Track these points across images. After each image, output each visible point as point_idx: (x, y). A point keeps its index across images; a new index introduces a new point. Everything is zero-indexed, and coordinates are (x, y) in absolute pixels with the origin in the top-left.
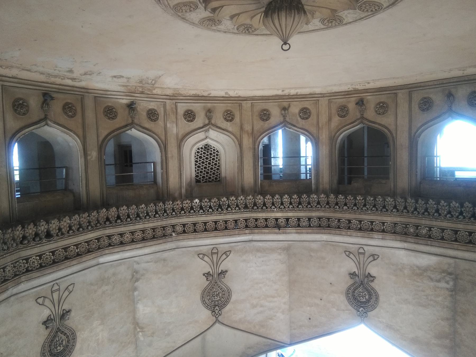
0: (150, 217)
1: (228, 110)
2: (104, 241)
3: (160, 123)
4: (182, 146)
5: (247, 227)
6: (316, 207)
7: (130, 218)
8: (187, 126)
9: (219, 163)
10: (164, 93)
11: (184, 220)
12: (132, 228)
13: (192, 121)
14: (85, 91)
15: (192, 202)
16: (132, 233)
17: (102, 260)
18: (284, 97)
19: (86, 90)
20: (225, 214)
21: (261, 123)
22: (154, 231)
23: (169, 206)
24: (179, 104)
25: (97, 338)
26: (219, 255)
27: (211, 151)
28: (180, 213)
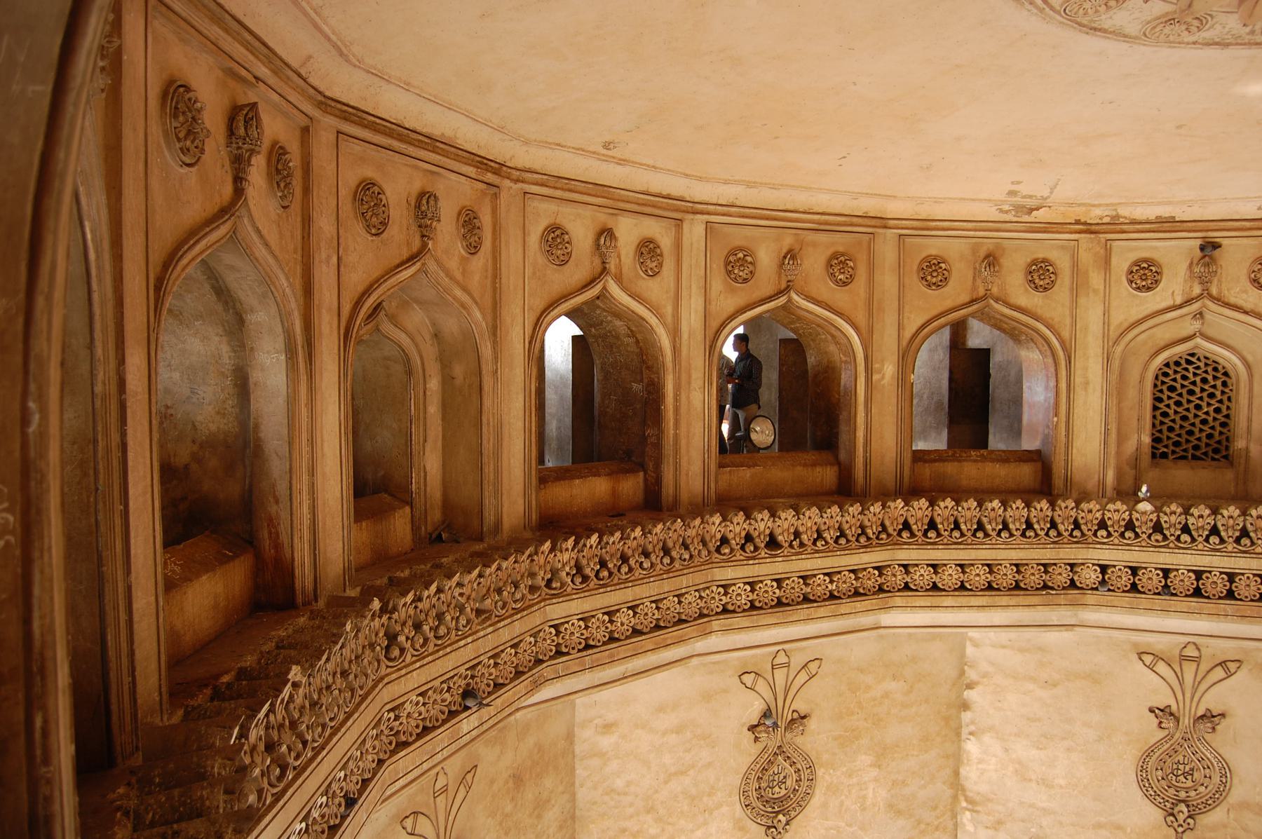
2: (894, 575)
3: (1061, 292)
7: (960, 530)
9: (1228, 408)
13: (1149, 289)
15: (1131, 509)
17: (887, 618)
20: (1229, 554)
22: (1018, 572)
26: (1204, 667)
28: (1095, 535)
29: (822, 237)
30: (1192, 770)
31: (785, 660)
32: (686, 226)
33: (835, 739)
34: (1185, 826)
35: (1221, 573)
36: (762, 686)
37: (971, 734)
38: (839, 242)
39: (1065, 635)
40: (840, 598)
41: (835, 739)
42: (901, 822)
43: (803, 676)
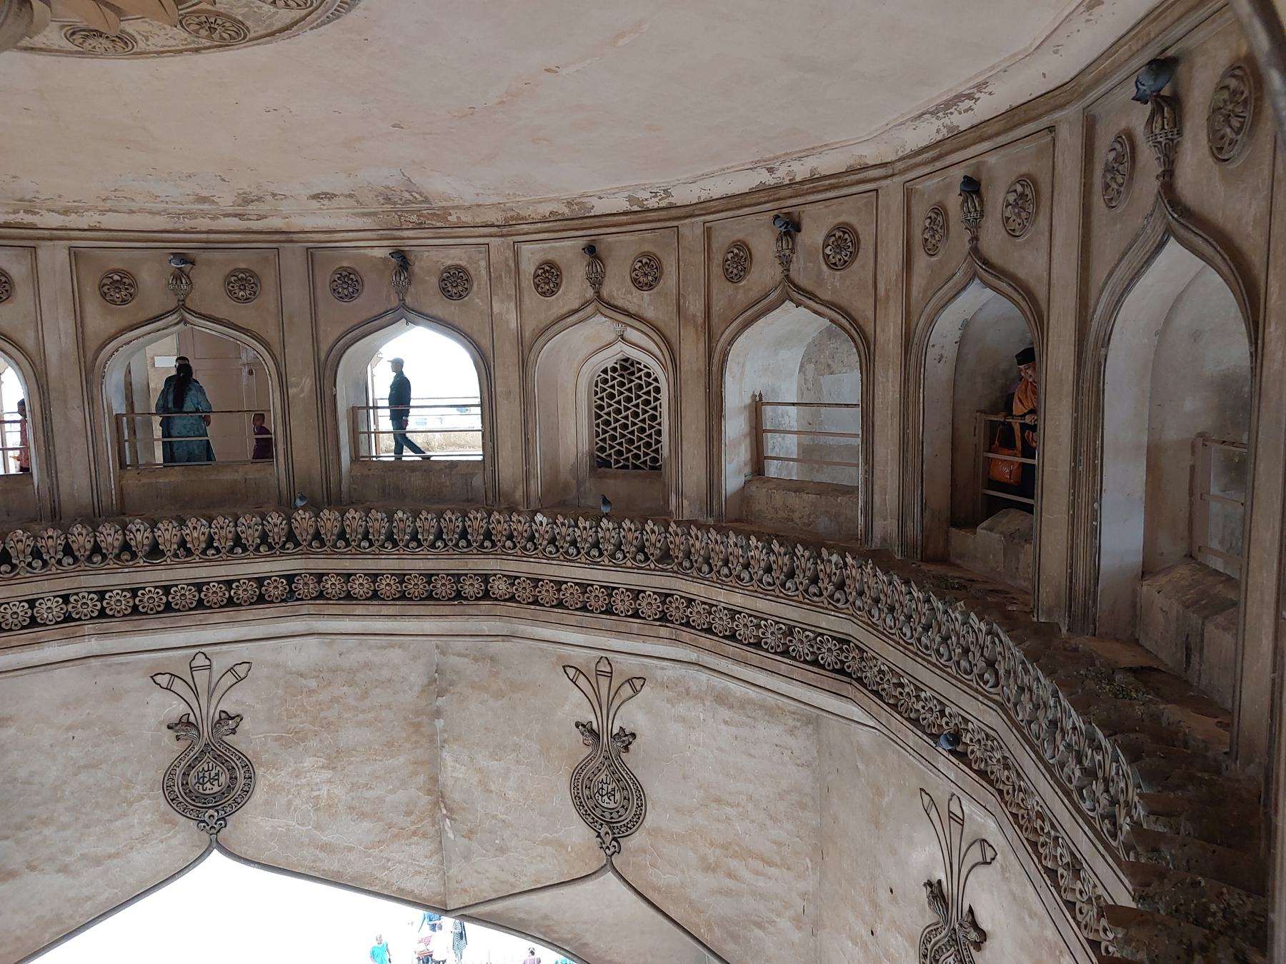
0: (420, 545)
1: (644, 254)
3: (477, 297)
4: (530, 363)
5: (664, 619)
6: (831, 596)
8: (540, 308)
10: (479, 220)
11: (512, 566)
12: (371, 565)
13: (553, 293)
14: (283, 237)
16: (374, 577)
18: (783, 193)
19: (286, 235)
21: (729, 288)
22: (429, 583)
23: (476, 524)
24: (525, 247)
25: (315, 794)
27: (640, 378)
29: (217, 255)
30: (613, 790)
31: (207, 663)
32: (39, 252)
33: (276, 739)
34: (612, 849)
35: (601, 587)
36: (178, 686)
37: (445, 741)
38: (242, 261)
39: (507, 644)
40: (240, 605)
41: (276, 739)
42: (366, 825)
43: (230, 679)
